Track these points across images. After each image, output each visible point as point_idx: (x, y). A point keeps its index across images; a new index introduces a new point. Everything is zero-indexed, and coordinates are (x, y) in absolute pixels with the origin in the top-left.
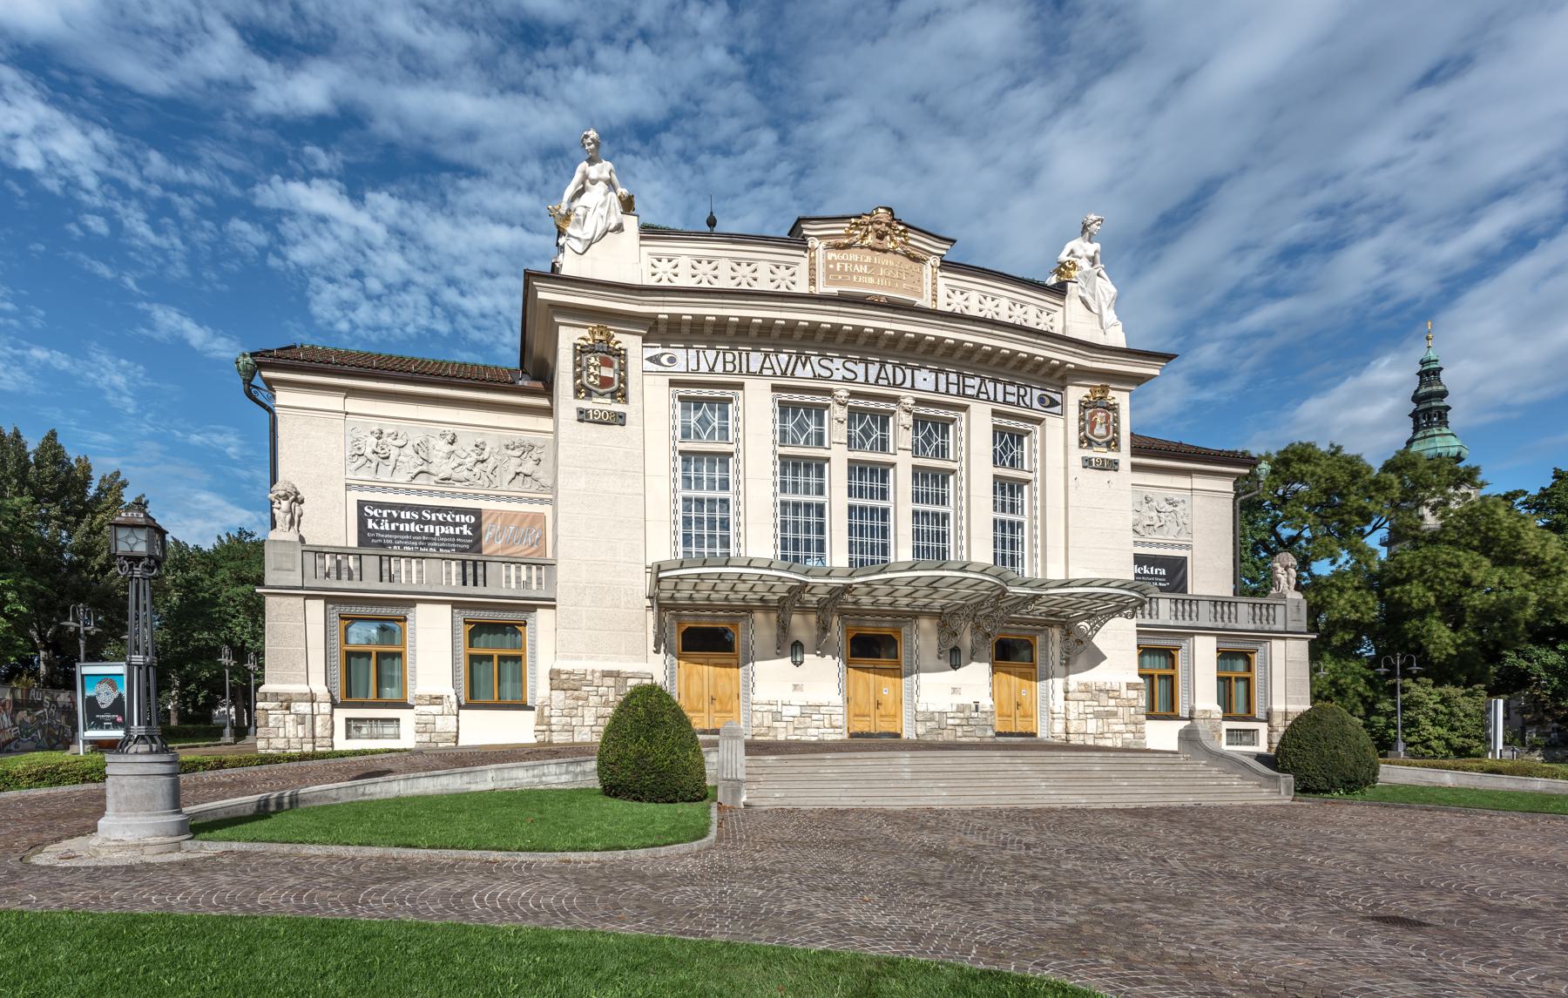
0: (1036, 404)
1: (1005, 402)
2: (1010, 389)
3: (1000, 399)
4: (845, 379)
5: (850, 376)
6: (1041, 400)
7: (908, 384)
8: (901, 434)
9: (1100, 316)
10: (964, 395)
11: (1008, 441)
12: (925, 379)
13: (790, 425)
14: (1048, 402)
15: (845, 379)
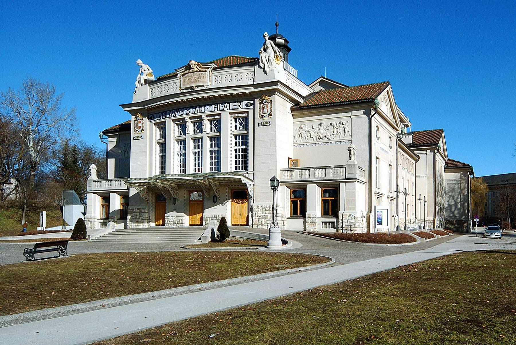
0: (245, 107)
1: (233, 109)
2: (234, 104)
3: (231, 108)
4: (187, 114)
5: (188, 112)
6: (247, 105)
7: (203, 111)
8: (207, 125)
9: (264, 69)
10: (219, 110)
11: (242, 120)
12: (208, 108)
13: (238, 124)
14: (249, 104)
15: (187, 114)
